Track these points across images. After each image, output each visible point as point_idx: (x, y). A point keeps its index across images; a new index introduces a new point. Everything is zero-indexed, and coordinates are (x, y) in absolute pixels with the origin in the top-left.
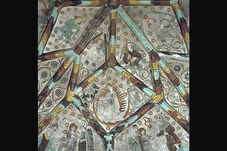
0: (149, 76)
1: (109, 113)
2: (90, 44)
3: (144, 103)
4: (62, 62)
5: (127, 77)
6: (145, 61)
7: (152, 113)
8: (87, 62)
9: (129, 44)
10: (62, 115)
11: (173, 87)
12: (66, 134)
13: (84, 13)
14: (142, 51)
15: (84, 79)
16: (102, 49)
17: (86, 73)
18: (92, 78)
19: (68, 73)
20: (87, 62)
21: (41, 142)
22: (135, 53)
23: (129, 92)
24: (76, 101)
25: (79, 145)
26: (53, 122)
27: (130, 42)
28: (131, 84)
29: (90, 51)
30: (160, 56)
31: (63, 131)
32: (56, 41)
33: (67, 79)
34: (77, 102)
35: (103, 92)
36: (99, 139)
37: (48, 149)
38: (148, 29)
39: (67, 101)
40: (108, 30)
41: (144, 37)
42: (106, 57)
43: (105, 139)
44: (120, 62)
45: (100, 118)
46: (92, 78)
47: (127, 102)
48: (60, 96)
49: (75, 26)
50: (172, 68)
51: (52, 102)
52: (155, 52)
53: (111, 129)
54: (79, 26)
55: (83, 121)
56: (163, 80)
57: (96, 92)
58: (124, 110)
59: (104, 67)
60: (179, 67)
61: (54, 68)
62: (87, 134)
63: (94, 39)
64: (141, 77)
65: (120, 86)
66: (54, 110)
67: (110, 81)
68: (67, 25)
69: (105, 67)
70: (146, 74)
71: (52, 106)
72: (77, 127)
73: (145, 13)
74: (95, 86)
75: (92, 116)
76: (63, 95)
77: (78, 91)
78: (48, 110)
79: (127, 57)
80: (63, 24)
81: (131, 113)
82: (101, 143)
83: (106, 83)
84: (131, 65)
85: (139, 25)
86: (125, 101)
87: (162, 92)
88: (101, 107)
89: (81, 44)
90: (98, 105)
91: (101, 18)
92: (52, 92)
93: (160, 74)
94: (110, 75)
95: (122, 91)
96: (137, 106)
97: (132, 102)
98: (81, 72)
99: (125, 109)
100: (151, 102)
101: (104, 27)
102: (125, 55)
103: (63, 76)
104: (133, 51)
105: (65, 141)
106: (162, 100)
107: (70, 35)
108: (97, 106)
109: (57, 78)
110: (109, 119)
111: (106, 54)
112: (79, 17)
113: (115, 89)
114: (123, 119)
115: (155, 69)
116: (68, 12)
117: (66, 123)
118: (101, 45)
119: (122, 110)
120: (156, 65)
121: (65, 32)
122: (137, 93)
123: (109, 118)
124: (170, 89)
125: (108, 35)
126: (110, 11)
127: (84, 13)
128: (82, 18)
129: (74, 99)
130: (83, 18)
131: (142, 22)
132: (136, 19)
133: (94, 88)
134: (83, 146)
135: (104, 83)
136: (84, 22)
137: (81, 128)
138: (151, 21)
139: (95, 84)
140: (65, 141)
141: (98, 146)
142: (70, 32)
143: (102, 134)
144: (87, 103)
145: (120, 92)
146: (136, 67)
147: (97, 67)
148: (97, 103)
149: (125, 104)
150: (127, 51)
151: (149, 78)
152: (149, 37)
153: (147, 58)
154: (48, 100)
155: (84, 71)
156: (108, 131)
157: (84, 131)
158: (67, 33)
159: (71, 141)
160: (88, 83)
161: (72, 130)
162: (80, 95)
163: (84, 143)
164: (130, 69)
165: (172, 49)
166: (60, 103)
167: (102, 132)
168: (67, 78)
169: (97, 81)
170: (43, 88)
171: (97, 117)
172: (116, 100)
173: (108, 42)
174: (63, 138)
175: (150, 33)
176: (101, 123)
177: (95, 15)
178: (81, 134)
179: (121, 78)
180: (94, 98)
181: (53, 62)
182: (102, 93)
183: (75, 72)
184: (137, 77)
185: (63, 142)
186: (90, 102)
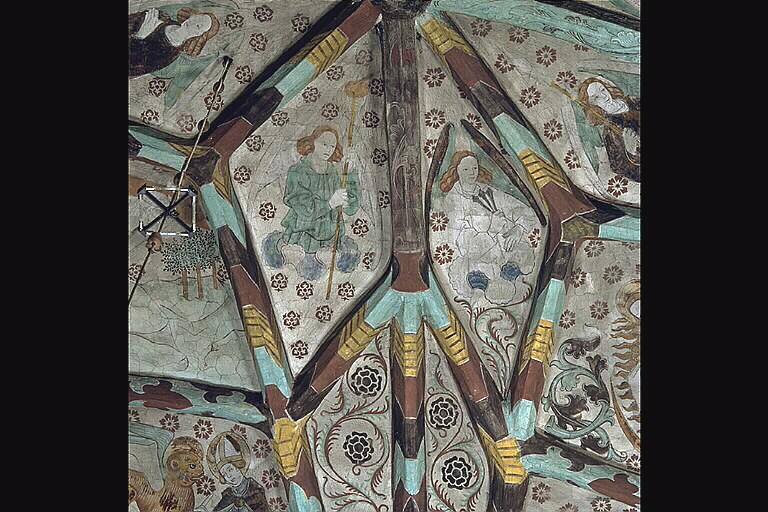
2: (436, 203)
4: (386, 353)
8: (478, 281)
9: (592, 90)
13: (319, 105)
16: (497, 186)
17: (506, 323)
18: (538, 338)
19: (436, 374)
20: (478, 281)
29: (455, 233)
32: (304, 291)
33: (451, 401)
34: (551, 464)
35: (625, 346)
39: (512, 489)
42: (535, 206)
44: (610, 190)
46: (538, 338)
49: (328, 181)
54: (339, 167)
57: (599, 364)
59: (556, 263)
61: (371, 399)
63: (434, 175)
67: (622, 282)
68: (293, 202)
74: (578, 347)
76: (477, 469)
77: (525, 419)
79: (623, 145)
80: (282, 211)
83: (612, 303)
89: (399, 243)
91: (398, 86)
92: (430, 491)
94: (606, 261)
98: (484, 336)
101: (439, 102)
102: (608, 141)
103: (430, 402)
107: (334, 227)
109: (412, 433)
111: (528, 196)
112: (315, 136)
116: (261, 153)
118: (483, 175)
121: (310, 233)
126: (411, 28)
127: (319, 105)
128: (330, 130)
129: (532, 462)
130: (332, 124)
133: (577, 356)
136: (350, 138)
142: (328, 219)
147: (531, 271)
150: (607, 122)
155: (492, 321)
158: (320, 231)
160: (539, 370)
162: (542, 424)
168: (445, 397)
169: (573, 322)
170: (390, 502)
177: (367, 82)
180: (604, 396)
181: (353, 377)
182: (623, 351)
183: (462, 358)
186: (602, 419)
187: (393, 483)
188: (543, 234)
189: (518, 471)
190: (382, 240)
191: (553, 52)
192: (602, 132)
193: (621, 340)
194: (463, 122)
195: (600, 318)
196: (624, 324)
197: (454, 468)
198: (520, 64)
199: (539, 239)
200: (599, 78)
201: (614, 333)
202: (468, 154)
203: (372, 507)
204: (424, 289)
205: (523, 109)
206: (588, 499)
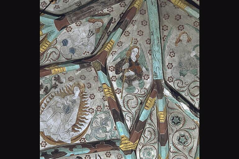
0: (135, 107)
1: (56, 124)
3: (108, 138)
5: (106, 93)
6: (142, 85)
7: (111, 155)
8: (65, 43)
9: (136, 49)
11: (156, 140)
14: (147, 70)
15: (48, 62)
16: (96, 35)
17: (56, 56)
20: (65, 43)
22: (135, 66)
23: (98, 112)
27: (139, 46)
28: (106, 103)
29: (77, 29)
30: (165, 94)
38: (174, 46)
40: (120, 15)
41: (160, 56)
42: (96, 49)
44: (110, 67)
46: (59, 69)
47: (88, 121)
50: (170, 116)
52: (161, 85)
53: (46, 147)
56: (150, 124)
57: (55, 86)
58: (78, 130)
59: (83, 62)
60: (180, 120)
64: (124, 102)
65: (91, 95)
67: (82, 81)
69: (85, 64)
70: (133, 103)
73: (183, 21)
74: (58, 79)
79: (124, 64)
81: (84, 139)
83: (74, 81)
84: (121, 78)
85: (166, 33)
86: (86, 119)
87: (138, 140)
88: (51, 110)
89: (70, 16)
90: (47, 105)
93: (151, 114)
95: (90, 103)
96: (98, 135)
97: (94, 125)
99: (79, 130)
100: (117, 144)
102: (123, 60)
104: (136, 61)
106: (132, 150)
108: (46, 105)
110: (51, 131)
111: (98, 45)
113: (82, 95)
114: (70, 142)
115: (147, 107)
118: (98, 30)
119: (76, 129)
120: (153, 102)
122: (107, 119)
124: (150, 141)
125: (115, 22)
131: (172, 31)
132: (166, 22)
133: (55, 80)
135: (73, 80)
138: (184, 38)
139: (59, 76)
145: (87, 104)
146: (126, 85)
147: (76, 57)
148: (48, 102)
149: (83, 123)
150: (128, 57)
151: (133, 111)
152: (168, 59)
153: (148, 84)
164: (117, 84)
165: (186, 92)
172: (76, 110)
173: (110, 31)
175: (172, 53)
179: (99, 87)
180: (47, 93)
182: (62, 91)
184: (119, 99)
188: (89, 55)
190: (65, 9)
191: (142, 35)
192: (125, 57)
193: (65, 89)
194: (112, 18)
195: (69, 80)
196: (70, 87)
198: (135, 27)
199: (86, 54)
200: (140, 50)
201: (66, 86)
202: (103, 23)
204: (58, 30)
205: (123, 34)
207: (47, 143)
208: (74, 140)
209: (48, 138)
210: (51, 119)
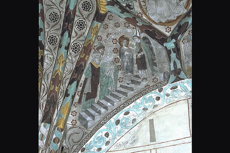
1: (164, 8)
10: (103, 32)
12: (117, 53)
21: (91, 73)
24: (112, 9)
25: (137, 62)
26: (95, 45)
31: (113, 51)
36: (160, 47)
37: (102, 78)
39: (101, 15)
43: (166, 47)
45: (152, 18)
48: (91, 9)
51: (84, 22)
53: (172, 30)
55: (133, 28)
62: (143, 44)
66: (90, 32)
71: (86, 26)
72: (129, 39)
75: (142, 20)
78: (84, 34)
82: (164, 53)
92: (77, 10)
105: (119, 62)
110: (166, 16)
114: (186, 11)
117: (113, 39)
123: (166, 14)
129: (109, 8)
134: (142, 62)
137: (134, 39)
140: (119, 62)
141: (161, 57)
143: (162, 40)
144: (130, 4)
154: (78, 22)
156: (168, 34)
157: (138, 41)
159: (126, 59)
161: (123, 45)
163: (143, 58)
166: (94, 19)
167: (160, 40)
170: (64, 10)
171: (149, 19)
174: (115, 59)
176: (157, 25)
178: (136, 47)
185: (117, 64)
187: (66, 5)
189: (104, 10)
197: (86, 4)
203: (59, 11)
206: (124, 22)
207: (170, 27)
208: (187, 5)
209: (168, 23)
210: (158, 8)
